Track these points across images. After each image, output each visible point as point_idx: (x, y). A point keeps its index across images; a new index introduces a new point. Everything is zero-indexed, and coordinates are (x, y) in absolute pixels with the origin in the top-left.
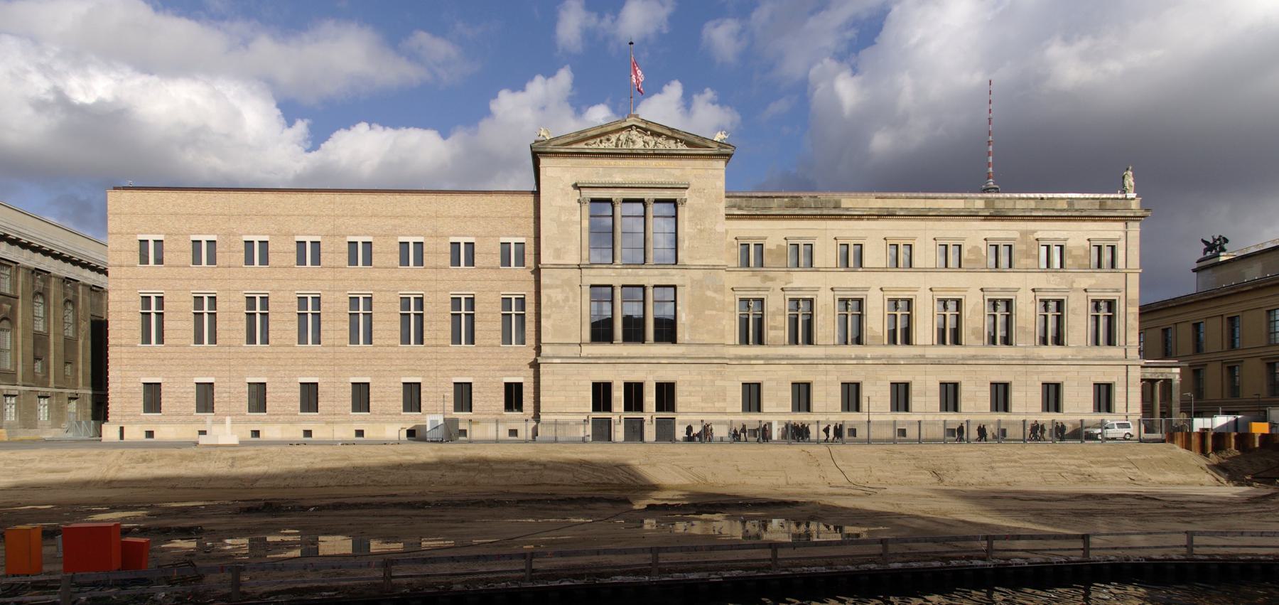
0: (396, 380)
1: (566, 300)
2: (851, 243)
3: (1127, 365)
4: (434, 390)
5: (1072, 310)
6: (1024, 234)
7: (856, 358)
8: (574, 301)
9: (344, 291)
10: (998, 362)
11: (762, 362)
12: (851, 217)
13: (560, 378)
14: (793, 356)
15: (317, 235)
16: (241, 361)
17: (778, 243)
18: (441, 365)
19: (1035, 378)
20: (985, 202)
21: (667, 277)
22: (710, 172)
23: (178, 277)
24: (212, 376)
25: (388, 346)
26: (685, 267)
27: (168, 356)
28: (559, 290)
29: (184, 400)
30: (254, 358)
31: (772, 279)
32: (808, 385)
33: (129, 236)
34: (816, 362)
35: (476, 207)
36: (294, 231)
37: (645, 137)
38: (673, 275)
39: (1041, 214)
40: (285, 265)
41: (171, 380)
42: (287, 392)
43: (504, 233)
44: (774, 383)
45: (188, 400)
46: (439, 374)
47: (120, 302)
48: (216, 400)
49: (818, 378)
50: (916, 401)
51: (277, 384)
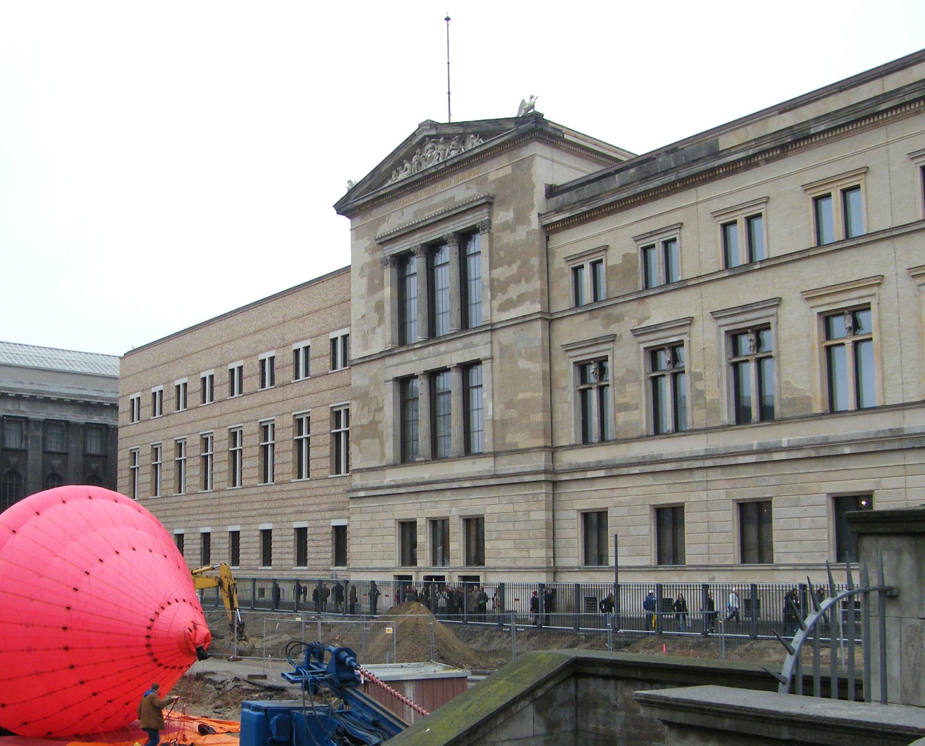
11: (602, 473)
13: (368, 517)
14: (652, 457)
21: (472, 349)
26: (491, 328)
31: (618, 319)
34: (685, 465)
37: (440, 147)
38: (477, 346)
44: (624, 511)
49: (694, 497)
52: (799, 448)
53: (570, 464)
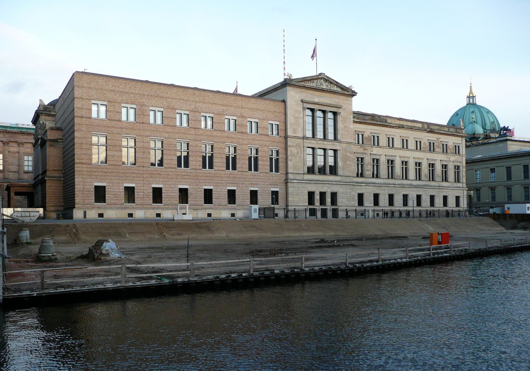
1: (298, 153)
2: (390, 137)
6: (438, 139)
7: (393, 184)
8: (301, 154)
11: (364, 185)
12: (391, 127)
13: (296, 189)
15: (187, 111)
16: (149, 175)
18: (245, 181)
22: (348, 102)
23: (115, 127)
24: (134, 183)
25: (221, 170)
27: (109, 170)
28: (295, 148)
29: (118, 196)
30: (156, 174)
31: (367, 150)
33: (87, 101)
34: (381, 185)
35: (258, 105)
36: (176, 108)
37: (327, 83)
38: (336, 145)
40: (171, 125)
41: (111, 184)
42: (173, 193)
45: (121, 196)
47: (82, 138)
48: (136, 196)
51: (168, 189)
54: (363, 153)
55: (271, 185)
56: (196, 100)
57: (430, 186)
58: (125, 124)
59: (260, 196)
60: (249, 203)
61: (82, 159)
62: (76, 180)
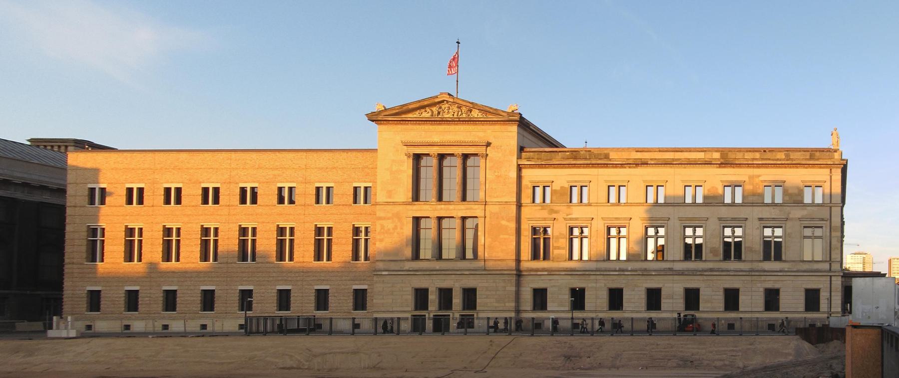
0: (273, 287)
3: (831, 276)
4: (301, 295)
5: (789, 234)
6: (751, 177)
7: (620, 270)
9: (236, 223)
10: (728, 273)
11: (546, 273)
12: (615, 166)
14: (571, 269)
15: (217, 183)
16: (159, 274)
17: (562, 185)
19: (759, 285)
20: (721, 154)
29: (117, 302)
31: (556, 212)
32: (582, 291)
34: (587, 273)
36: (201, 180)
39: (760, 163)
41: (108, 288)
42: (192, 297)
43: (357, 180)
45: (120, 302)
46: (305, 283)
50: (665, 303)
51: (185, 291)
52: (636, 271)
53: (528, 268)
54: (545, 219)
55: (352, 280)
56: (232, 166)
57: (722, 271)
58: (129, 209)
59: (333, 298)
60: (313, 308)
61: (73, 258)
62: (65, 284)
